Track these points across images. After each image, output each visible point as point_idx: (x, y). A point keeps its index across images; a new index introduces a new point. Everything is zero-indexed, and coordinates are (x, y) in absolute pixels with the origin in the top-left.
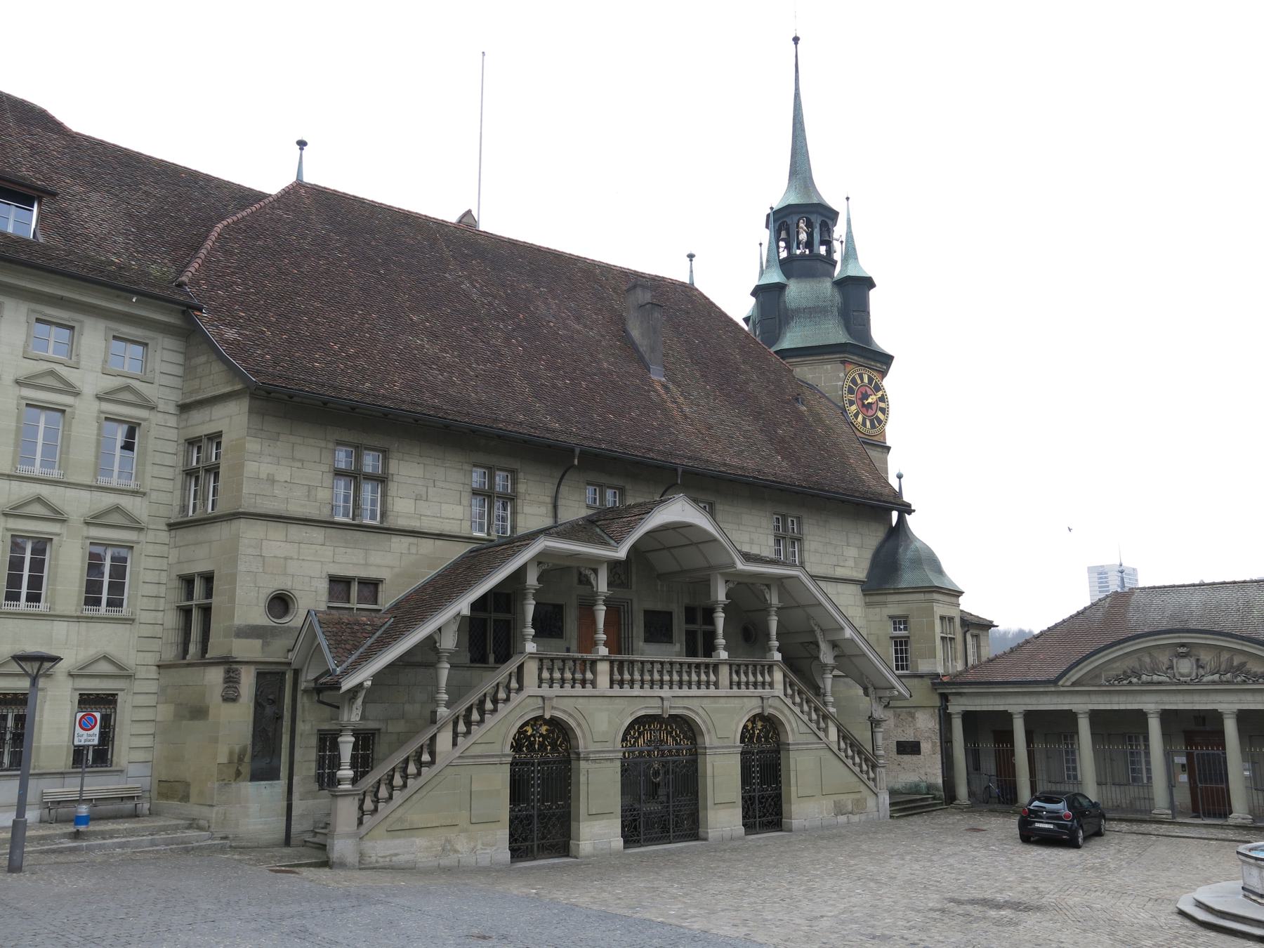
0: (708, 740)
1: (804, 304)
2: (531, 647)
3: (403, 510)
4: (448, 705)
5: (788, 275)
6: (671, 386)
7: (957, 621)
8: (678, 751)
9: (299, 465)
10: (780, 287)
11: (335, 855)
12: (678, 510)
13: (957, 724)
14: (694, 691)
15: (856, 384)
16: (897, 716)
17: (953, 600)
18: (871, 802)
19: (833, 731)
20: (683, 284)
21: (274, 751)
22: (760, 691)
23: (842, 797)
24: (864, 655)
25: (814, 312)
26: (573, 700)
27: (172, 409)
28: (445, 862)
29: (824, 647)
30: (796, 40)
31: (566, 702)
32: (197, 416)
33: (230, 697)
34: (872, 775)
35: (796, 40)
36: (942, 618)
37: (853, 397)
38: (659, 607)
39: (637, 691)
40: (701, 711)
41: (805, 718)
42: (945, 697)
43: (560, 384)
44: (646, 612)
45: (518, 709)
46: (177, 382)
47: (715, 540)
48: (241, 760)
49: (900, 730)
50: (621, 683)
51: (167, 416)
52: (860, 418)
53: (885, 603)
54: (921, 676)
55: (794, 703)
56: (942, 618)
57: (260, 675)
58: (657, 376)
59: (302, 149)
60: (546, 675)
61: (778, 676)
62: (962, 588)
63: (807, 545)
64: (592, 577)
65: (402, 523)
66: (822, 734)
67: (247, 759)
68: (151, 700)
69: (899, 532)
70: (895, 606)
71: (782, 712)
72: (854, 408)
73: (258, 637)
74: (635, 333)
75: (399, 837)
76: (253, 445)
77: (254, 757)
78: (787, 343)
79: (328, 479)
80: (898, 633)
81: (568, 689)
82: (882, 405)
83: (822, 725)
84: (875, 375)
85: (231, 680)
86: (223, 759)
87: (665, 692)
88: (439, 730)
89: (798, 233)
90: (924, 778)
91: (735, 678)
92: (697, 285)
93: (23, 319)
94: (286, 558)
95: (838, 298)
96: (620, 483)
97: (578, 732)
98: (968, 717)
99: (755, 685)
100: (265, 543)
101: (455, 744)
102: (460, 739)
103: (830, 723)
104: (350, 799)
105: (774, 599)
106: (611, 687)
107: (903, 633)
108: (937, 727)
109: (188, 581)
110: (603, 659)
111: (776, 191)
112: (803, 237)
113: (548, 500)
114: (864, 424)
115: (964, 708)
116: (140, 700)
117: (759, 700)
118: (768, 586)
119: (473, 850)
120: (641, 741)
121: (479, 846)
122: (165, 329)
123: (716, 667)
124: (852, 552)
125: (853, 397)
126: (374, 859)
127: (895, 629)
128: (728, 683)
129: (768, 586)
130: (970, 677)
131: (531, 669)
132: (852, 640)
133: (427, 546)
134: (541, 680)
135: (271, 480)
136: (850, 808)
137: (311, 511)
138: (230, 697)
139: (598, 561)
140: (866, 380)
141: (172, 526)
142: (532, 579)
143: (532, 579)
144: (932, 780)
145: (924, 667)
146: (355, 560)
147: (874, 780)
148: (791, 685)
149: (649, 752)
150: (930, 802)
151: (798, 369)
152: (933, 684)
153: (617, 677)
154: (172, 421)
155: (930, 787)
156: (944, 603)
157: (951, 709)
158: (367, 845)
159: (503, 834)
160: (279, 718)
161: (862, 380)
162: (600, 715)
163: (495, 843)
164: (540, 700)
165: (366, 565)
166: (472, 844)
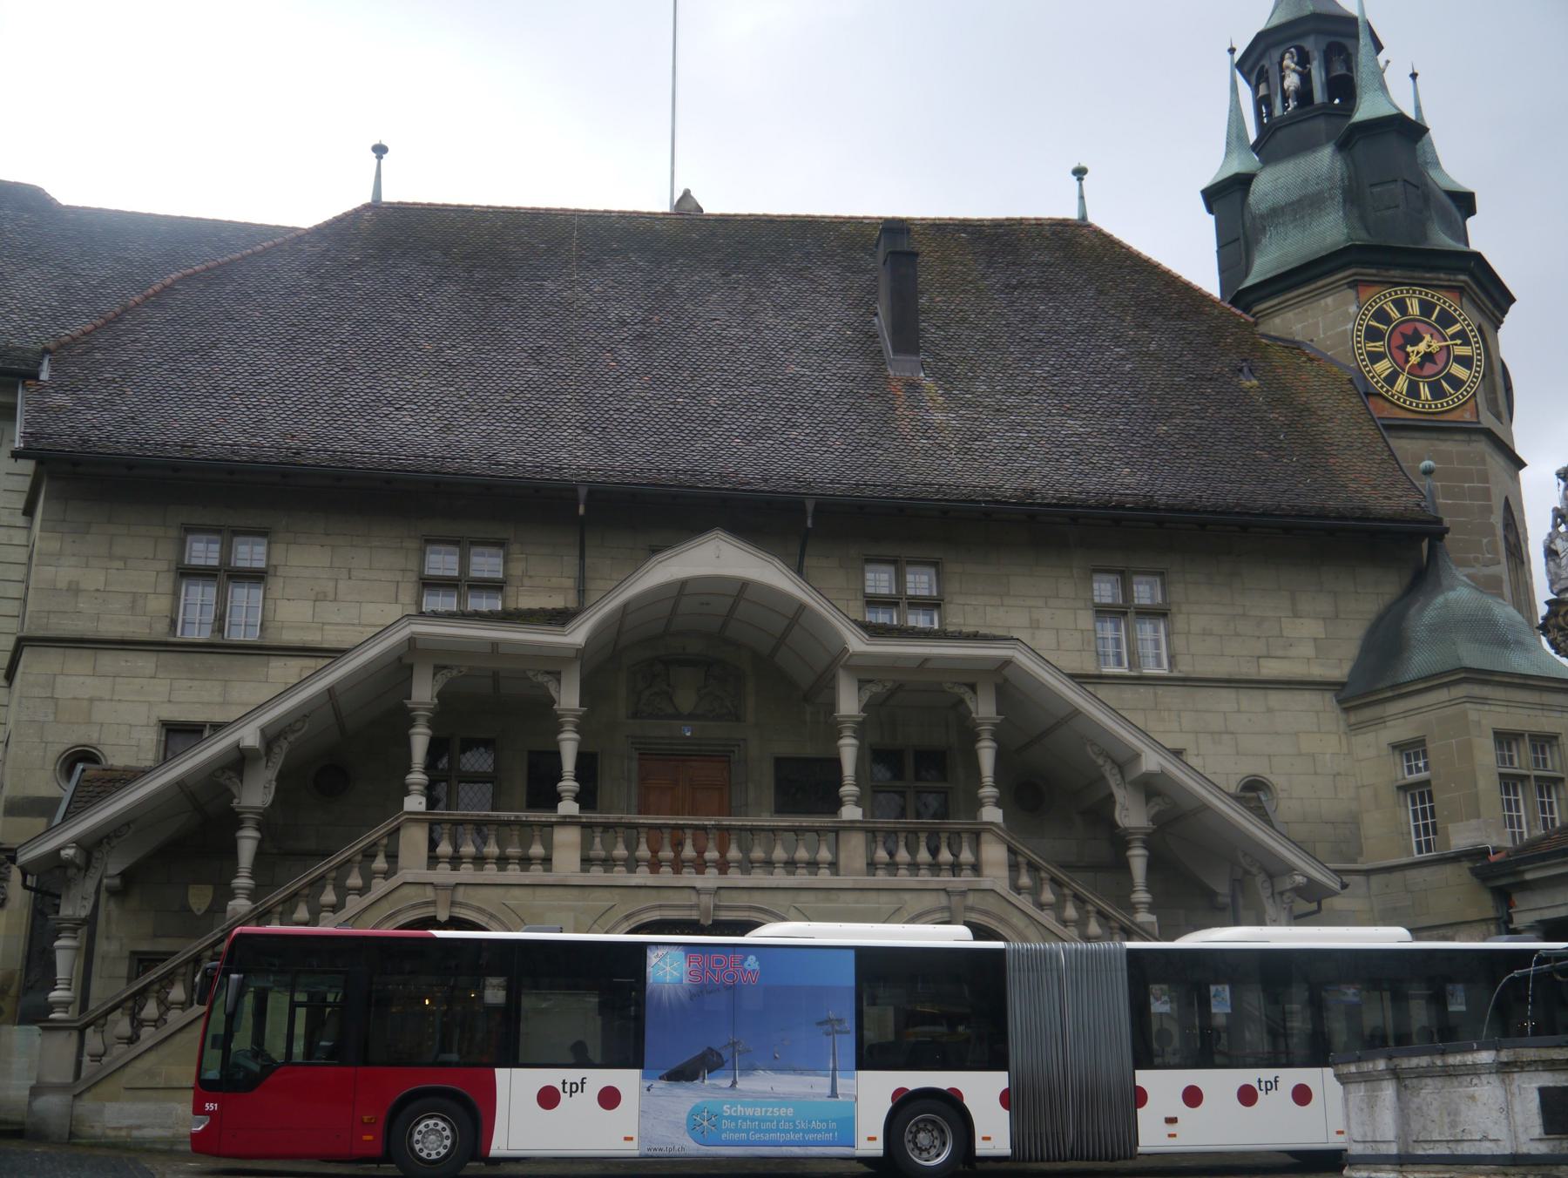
1: (1281, 198)
2: (415, 803)
4: (253, 895)
9: (120, 564)
12: (716, 558)
20: (1064, 224)
22: (945, 879)
25: (1302, 207)
26: (500, 891)
27: (21, 520)
29: (1121, 795)
36: (1504, 739)
37: (1378, 346)
39: (642, 877)
44: (779, 762)
47: (802, 607)
51: (12, 531)
52: (1402, 383)
53: (1381, 721)
56: (1504, 739)
59: (379, 158)
60: (445, 848)
61: (994, 853)
65: (290, 637)
71: (1001, 920)
72: (1383, 367)
73: (42, 814)
80: (1415, 777)
81: (491, 873)
87: (711, 879)
89: (1283, 78)
92: (1091, 219)
94: (91, 700)
99: (935, 868)
100: (59, 679)
104: (64, 1034)
105: (984, 708)
107: (1423, 775)
110: (567, 822)
112: (1292, 81)
113: (570, 583)
114: (1413, 391)
115: (1537, 916)
118: (973, 687)
124: (1310, 628)
127: (1409, 768)
128: (860, 863)
129: (973, 687)
131: (414, 841)
132: (1163, 774)
134: (433, 860)
135: (74, 590)
140: (1414, 308)
142: (424, 692)
143: (424, 692)
145: (1461, 837)
146: (193, 696)
148: (1033, 868)
151: (1277, 321)
156: (1508, 703)
165: (225, 703)
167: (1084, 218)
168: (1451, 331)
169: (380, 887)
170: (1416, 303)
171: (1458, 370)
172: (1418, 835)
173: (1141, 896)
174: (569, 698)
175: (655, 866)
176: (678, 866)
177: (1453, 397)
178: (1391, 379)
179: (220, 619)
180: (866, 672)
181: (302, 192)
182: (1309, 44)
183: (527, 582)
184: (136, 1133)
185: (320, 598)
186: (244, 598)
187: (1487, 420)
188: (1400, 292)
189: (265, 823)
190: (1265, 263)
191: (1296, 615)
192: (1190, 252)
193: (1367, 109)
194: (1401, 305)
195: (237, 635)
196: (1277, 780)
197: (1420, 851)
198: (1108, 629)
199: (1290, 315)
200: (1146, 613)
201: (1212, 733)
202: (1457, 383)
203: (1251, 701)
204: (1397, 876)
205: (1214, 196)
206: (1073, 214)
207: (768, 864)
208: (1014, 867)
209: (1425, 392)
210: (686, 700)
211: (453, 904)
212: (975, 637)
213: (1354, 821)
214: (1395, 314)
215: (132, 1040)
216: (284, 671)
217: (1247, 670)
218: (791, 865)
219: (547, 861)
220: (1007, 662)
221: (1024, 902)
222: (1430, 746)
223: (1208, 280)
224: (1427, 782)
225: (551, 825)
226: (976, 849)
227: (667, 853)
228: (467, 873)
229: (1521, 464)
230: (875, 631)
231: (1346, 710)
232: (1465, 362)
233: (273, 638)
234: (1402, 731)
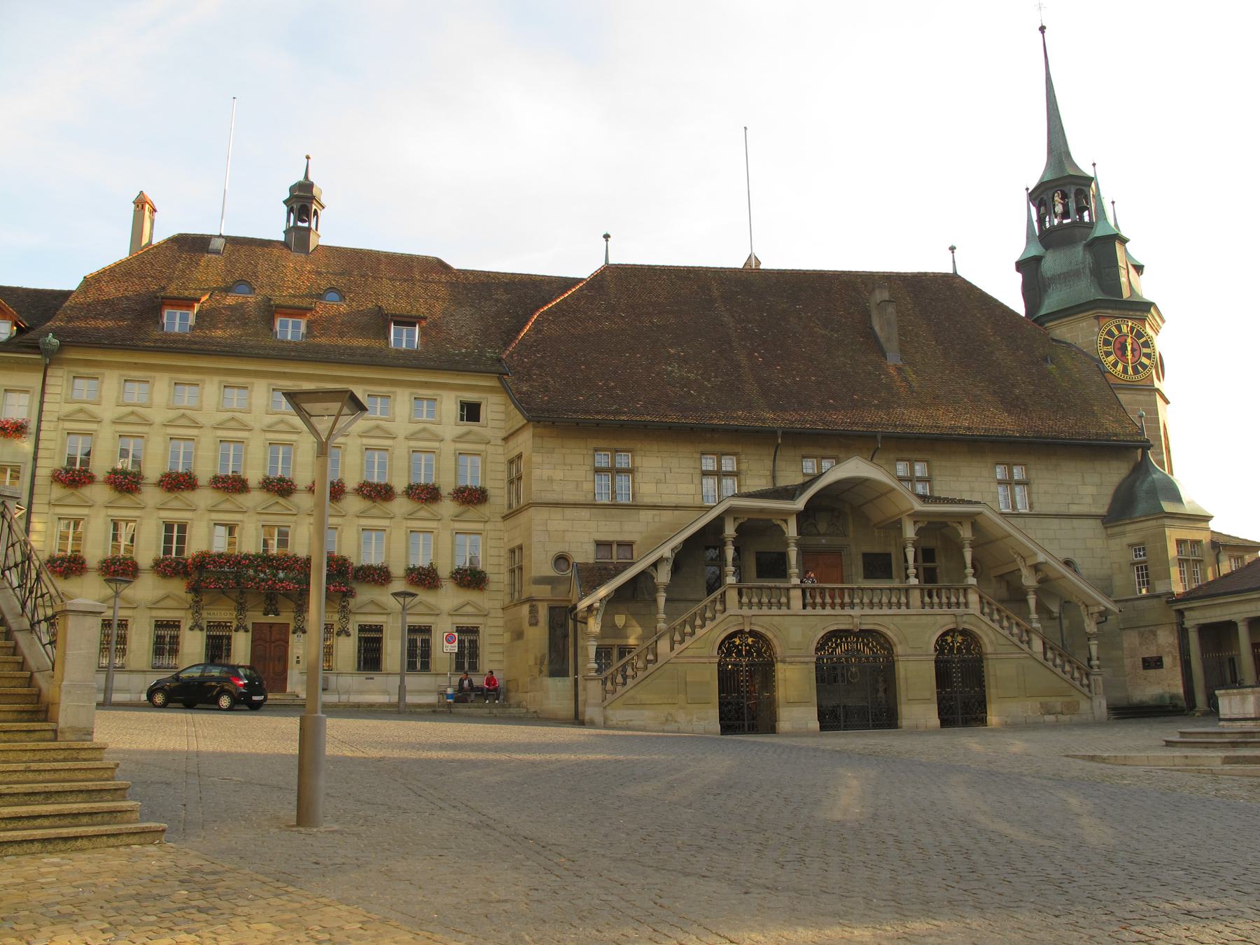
0: (899, 649)
2: (731, 580)
3: (648, 491)
5: (1047, 247)
6: (907, 368)
8: (875, 658)
10: (1037, 260)
11: (587, 718)
12: (855, 468)
13: (1193, 638)
14: (885, 611)
16: (1141, 635)
17: (1202, 525)
18: (1084, 705)
19: (1037, 645)
20: (946, 275)
21: (564, 659)
22: (954, 610)
24: (1064, 577)
25: (1067, 277)
27: (500, 442)
29: (1025, 572)
30: (1042, 29)
31: (763, 619)
32: (512, 443)
33: (534, 623)
34: (1085, 681)
35: (1042, 29)
36: (1180, 543)
37: (1110, 348)
38: (877, 549)
39: (828, 611)
40: (892, 627)
41: (1006, 632)
42: (1180, 613)
43: (788, 381)
44: (865, 555)
46: (502, 424)
47: (893, 489)
48: (542, 663)
50: (814, 606)
52: (1120, 367)
53: (1123, 533)
54: (1158, 596)
55: (993, 621)
56: (1180, 543)
57: (551, 609)
58: (893, 359)
60: (745, 600)
61: (973, 598)
62: (1210, 512)
63: (1034, 488)
64: (784, 526)
65: (648, 500)
66: (1025, 646)
67: (546, 662)
68: (500, 631)
69: (1142, 468)
70: (1133, 532)
72: (1112, 358)
74: (877, 328)
76: (537, 458)
77: (551, 662)
78: (1043, 312)
79: (590, 475)
81: (765, 610)
82: (1145, 350)
83: (1025, 638)
84: (1138, 326)
85: (533, 611)
86: (531, 662)
87: (856, 612)
88: (659, 638)
90: (1167, 689)
91: (927, 599)
93: (406, 398)
95: (1089, 259)
96: (834, 453)
97: (775, 642)
98: (1204, 629)
99: (949, 605)
101: (672, 649)
102: (676, 646)
103: (1033, 636)
105: (966, 533)
106: (804, 607)
109: (512, 551)
110: (795, 587)
111: (1034, 169)
112: (1059, 209)
114: (1125, 371)
115: (1196, 622)
116: (494, 631)
120: (838, 650)
122: (491, 390)
123: (907, 590)
125: (1110, 348)
128: (919, 603)
130: (1201, 593)
131: (732, 596)
133: (667, 516)
134: (741, 605)
135: (551, 480)
136: (1059, 709)
137: (580, 498)
138: (534, 623)
139: (789, 513)
141: (505, 518)
142: (730, 530)
143: (730, 530)
145: (1160, 588)
146: (611, 529)
147: (1089, 686)
149: (847, 660)
152: (1168, 602)
153: (809, 600)
154: (500, 450)
155: (1173, 697)
157: (1188, 624)
158: (609, 712)
159: (714, 713)
160: (566, 636)
161: (1119, 329)
162: (795, 629)
163: (711, 718)
164: (741, 619)
167: (955, 273)
169: (720, 617)
171: (1144, 360)
173: (1034, 616)
174: (791, 530)
175: (833, 606)
176: (843, 606)
179: (614, 492)
180: (916, 517)
181: (581, 264)
182: (1066, 189)
185: (658, 482)
186: (623, 482)
188: (1118, 321)
189: (668, 589)
190: (1051, 303)
191: (1084, 484)
192: (1008, 291)
193: (1099, 232)
194: (1119, 328)
195: (623, 500)
196: (1077, 561)
198: (1000, 489)
202: (1144, 366)
203: (1065, 523)
205: (1020, 266)
206: (951, 271)
207: (880, 605)
208: (981, 601)
209: (1130, 370)
210: (822, 527)
212: (962, 502)
213: (1110, 578)
214: (1116, 333)
215: (624, 684)
216: (646, 515)
217: (1063, 510)
218: (890, 605)
219: (788, 606)
220: (979, 513)
221: (986, 619)
222: (1147, 547)
223: (1019, 307)
225: (788, 589)
226: (965, 596)
227: (838, 601)
228: (755, 610)
230: (923, 498)
232: (1148, 356)
233: (639, 501)
234: (1132, 538)
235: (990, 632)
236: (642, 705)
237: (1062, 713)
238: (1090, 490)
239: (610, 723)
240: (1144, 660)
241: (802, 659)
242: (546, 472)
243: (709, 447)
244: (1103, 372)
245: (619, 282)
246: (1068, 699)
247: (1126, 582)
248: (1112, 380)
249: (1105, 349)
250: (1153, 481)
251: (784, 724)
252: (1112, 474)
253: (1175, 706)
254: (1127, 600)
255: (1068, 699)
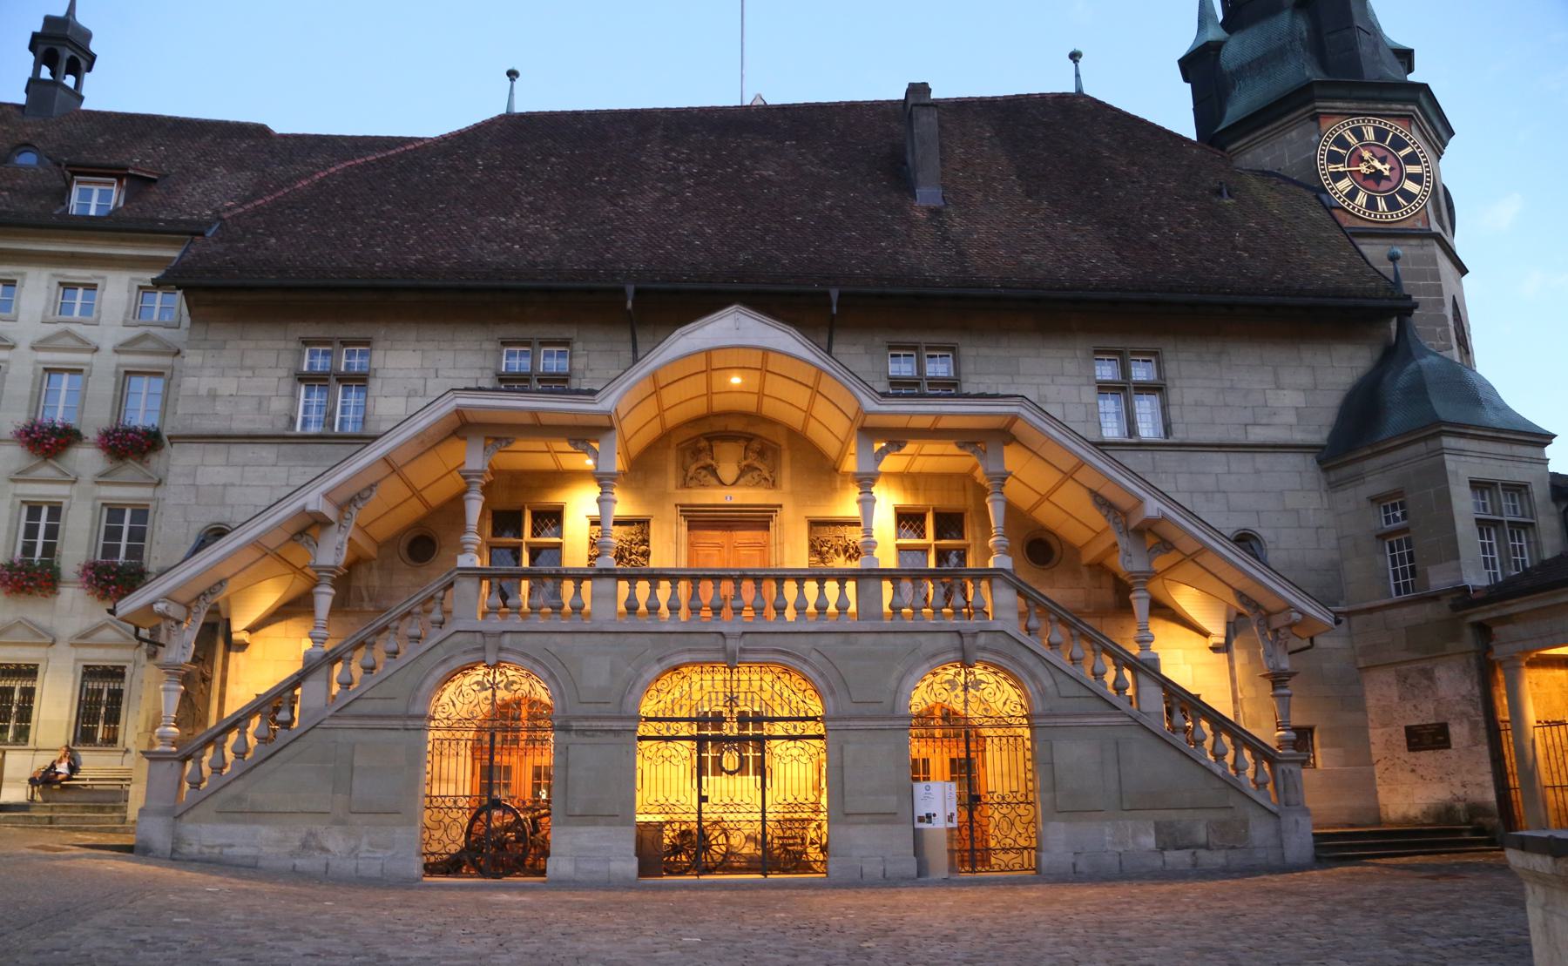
7: (1540, 492)
9: (250, 373)
15: (1347, 145)
16: (1403, 679)
17: (1529, 451)
18: (1260, 831)
20: (1063, 96)
23: (1173, 815)
26: (544, 637)
28: (300, 863)
36: (1477, 486)
42: (1483, 630)
45: (439, 649)
49: (1409, 706)
52: (1361, 198)
53: (1358, 478)
54: (1435, 597)
56: (1477, 486)
63: (1174, 395)
69: (1396, 353)
70: (1377, 476)
72: (1345, 185)
75: (234, 822)
82: (1411, 169)
90: (1460, 792)
92: (1086, 92)
94: (225, 486)
107: (1402, 523)
108: (1477, 691)
117: (956, 641)
119: (353, 852)
121: (364, 847)
124: (1290, 399)
126: (195, 849)
127: (1387, 519)
135: (213, 396)
140: (1370, 135)
144: (1475, 795)
145: (1438, 579)
150: (1467, 836)
155: (1475, 809)
158: (188, 827)
166: (352, 843)
168: (1403, 153)
170: (1371, 130)
172: (1396, 578)
177: (1407, 210)
178: (1352, 195)
183: (588, 374)
184: (226, 850)
187: (1435, 228)
190: (1236, 110)
191: (1279, 387)
192: (1172, 109)
194: (1358, 133)
196: (1265, 533)
197: (1398, 593)
199: (1260, 150)
200: (1144, 388)
201: (1206, 493)
202: (1410, 197)
203: (1242, 464)
204: (1377, 615)
206: (1072, 89)
209: (1382, 204)
210: (728, 471)
211: (501, 649)
214: (1352, 140)
217: (1236, 436)
224: (1405, 530)
229: (1463, 270)
231: (1326, 470)
232: (1416, 179)
234: (1377, 484)
235: (1040, 671)
236: (256, 814)
237: (1207, 847)
238: (1290, 399)
239: (185, 849)
240: (1410, 731)
241: (606, 724)
242: (204, 383)
243: (514, 331)
244: (1330, 208)
245: (517, 136)
246: (1223, 815)
247: (1371, 576)
248: (1347, 222)
249: (1332, 168)
250: (1419, 370)
251: (558, 865)
252: (1337, 370)
253: (1480, 830)
254: (1370, 610)
255: (1223, 815)
